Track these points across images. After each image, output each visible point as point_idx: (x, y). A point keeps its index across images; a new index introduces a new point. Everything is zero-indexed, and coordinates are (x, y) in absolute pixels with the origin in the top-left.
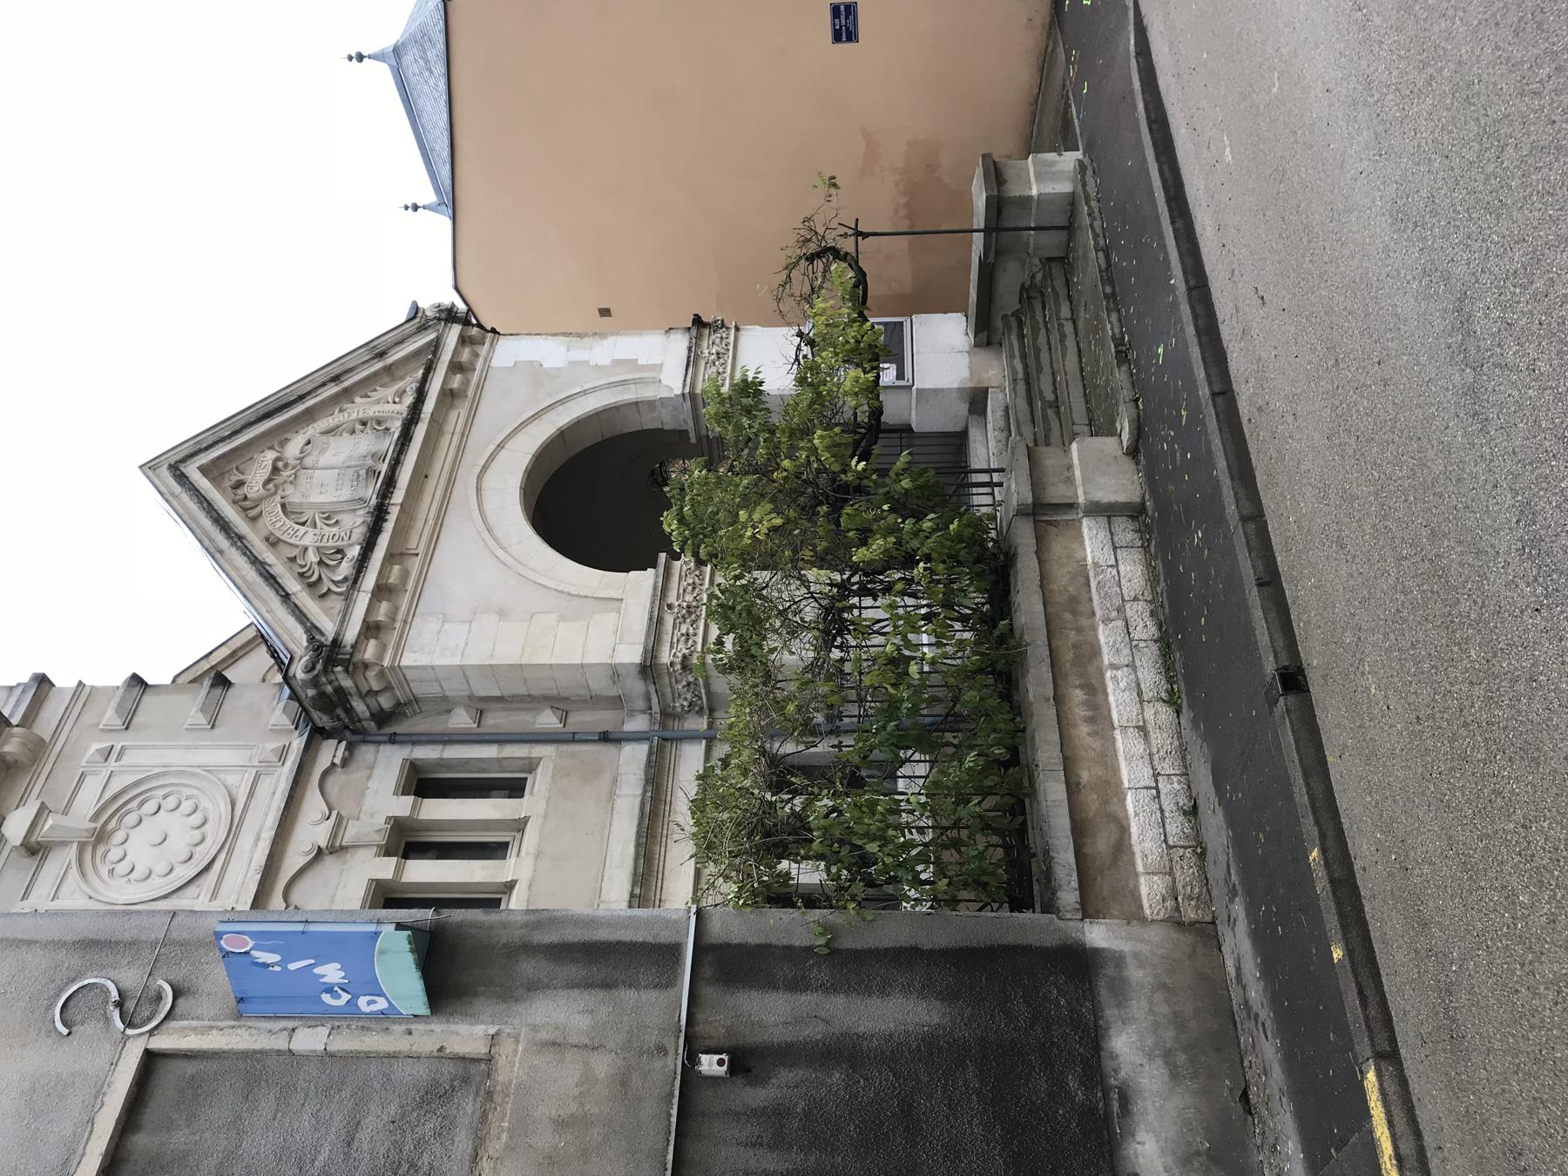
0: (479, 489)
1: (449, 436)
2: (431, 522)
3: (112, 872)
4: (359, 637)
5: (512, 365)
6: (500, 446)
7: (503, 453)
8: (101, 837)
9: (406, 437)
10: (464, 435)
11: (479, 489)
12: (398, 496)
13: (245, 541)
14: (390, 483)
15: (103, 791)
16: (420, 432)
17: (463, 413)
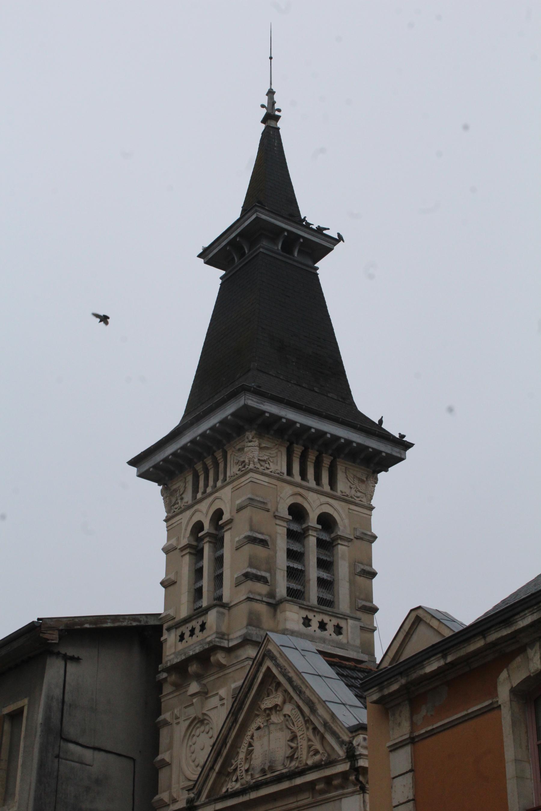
1: (295, 800)
3: (194, 735)
12: (253, 795)
14: (257, 786)
15: (212, 709)
16: (285, 785)
17: (310, 800)
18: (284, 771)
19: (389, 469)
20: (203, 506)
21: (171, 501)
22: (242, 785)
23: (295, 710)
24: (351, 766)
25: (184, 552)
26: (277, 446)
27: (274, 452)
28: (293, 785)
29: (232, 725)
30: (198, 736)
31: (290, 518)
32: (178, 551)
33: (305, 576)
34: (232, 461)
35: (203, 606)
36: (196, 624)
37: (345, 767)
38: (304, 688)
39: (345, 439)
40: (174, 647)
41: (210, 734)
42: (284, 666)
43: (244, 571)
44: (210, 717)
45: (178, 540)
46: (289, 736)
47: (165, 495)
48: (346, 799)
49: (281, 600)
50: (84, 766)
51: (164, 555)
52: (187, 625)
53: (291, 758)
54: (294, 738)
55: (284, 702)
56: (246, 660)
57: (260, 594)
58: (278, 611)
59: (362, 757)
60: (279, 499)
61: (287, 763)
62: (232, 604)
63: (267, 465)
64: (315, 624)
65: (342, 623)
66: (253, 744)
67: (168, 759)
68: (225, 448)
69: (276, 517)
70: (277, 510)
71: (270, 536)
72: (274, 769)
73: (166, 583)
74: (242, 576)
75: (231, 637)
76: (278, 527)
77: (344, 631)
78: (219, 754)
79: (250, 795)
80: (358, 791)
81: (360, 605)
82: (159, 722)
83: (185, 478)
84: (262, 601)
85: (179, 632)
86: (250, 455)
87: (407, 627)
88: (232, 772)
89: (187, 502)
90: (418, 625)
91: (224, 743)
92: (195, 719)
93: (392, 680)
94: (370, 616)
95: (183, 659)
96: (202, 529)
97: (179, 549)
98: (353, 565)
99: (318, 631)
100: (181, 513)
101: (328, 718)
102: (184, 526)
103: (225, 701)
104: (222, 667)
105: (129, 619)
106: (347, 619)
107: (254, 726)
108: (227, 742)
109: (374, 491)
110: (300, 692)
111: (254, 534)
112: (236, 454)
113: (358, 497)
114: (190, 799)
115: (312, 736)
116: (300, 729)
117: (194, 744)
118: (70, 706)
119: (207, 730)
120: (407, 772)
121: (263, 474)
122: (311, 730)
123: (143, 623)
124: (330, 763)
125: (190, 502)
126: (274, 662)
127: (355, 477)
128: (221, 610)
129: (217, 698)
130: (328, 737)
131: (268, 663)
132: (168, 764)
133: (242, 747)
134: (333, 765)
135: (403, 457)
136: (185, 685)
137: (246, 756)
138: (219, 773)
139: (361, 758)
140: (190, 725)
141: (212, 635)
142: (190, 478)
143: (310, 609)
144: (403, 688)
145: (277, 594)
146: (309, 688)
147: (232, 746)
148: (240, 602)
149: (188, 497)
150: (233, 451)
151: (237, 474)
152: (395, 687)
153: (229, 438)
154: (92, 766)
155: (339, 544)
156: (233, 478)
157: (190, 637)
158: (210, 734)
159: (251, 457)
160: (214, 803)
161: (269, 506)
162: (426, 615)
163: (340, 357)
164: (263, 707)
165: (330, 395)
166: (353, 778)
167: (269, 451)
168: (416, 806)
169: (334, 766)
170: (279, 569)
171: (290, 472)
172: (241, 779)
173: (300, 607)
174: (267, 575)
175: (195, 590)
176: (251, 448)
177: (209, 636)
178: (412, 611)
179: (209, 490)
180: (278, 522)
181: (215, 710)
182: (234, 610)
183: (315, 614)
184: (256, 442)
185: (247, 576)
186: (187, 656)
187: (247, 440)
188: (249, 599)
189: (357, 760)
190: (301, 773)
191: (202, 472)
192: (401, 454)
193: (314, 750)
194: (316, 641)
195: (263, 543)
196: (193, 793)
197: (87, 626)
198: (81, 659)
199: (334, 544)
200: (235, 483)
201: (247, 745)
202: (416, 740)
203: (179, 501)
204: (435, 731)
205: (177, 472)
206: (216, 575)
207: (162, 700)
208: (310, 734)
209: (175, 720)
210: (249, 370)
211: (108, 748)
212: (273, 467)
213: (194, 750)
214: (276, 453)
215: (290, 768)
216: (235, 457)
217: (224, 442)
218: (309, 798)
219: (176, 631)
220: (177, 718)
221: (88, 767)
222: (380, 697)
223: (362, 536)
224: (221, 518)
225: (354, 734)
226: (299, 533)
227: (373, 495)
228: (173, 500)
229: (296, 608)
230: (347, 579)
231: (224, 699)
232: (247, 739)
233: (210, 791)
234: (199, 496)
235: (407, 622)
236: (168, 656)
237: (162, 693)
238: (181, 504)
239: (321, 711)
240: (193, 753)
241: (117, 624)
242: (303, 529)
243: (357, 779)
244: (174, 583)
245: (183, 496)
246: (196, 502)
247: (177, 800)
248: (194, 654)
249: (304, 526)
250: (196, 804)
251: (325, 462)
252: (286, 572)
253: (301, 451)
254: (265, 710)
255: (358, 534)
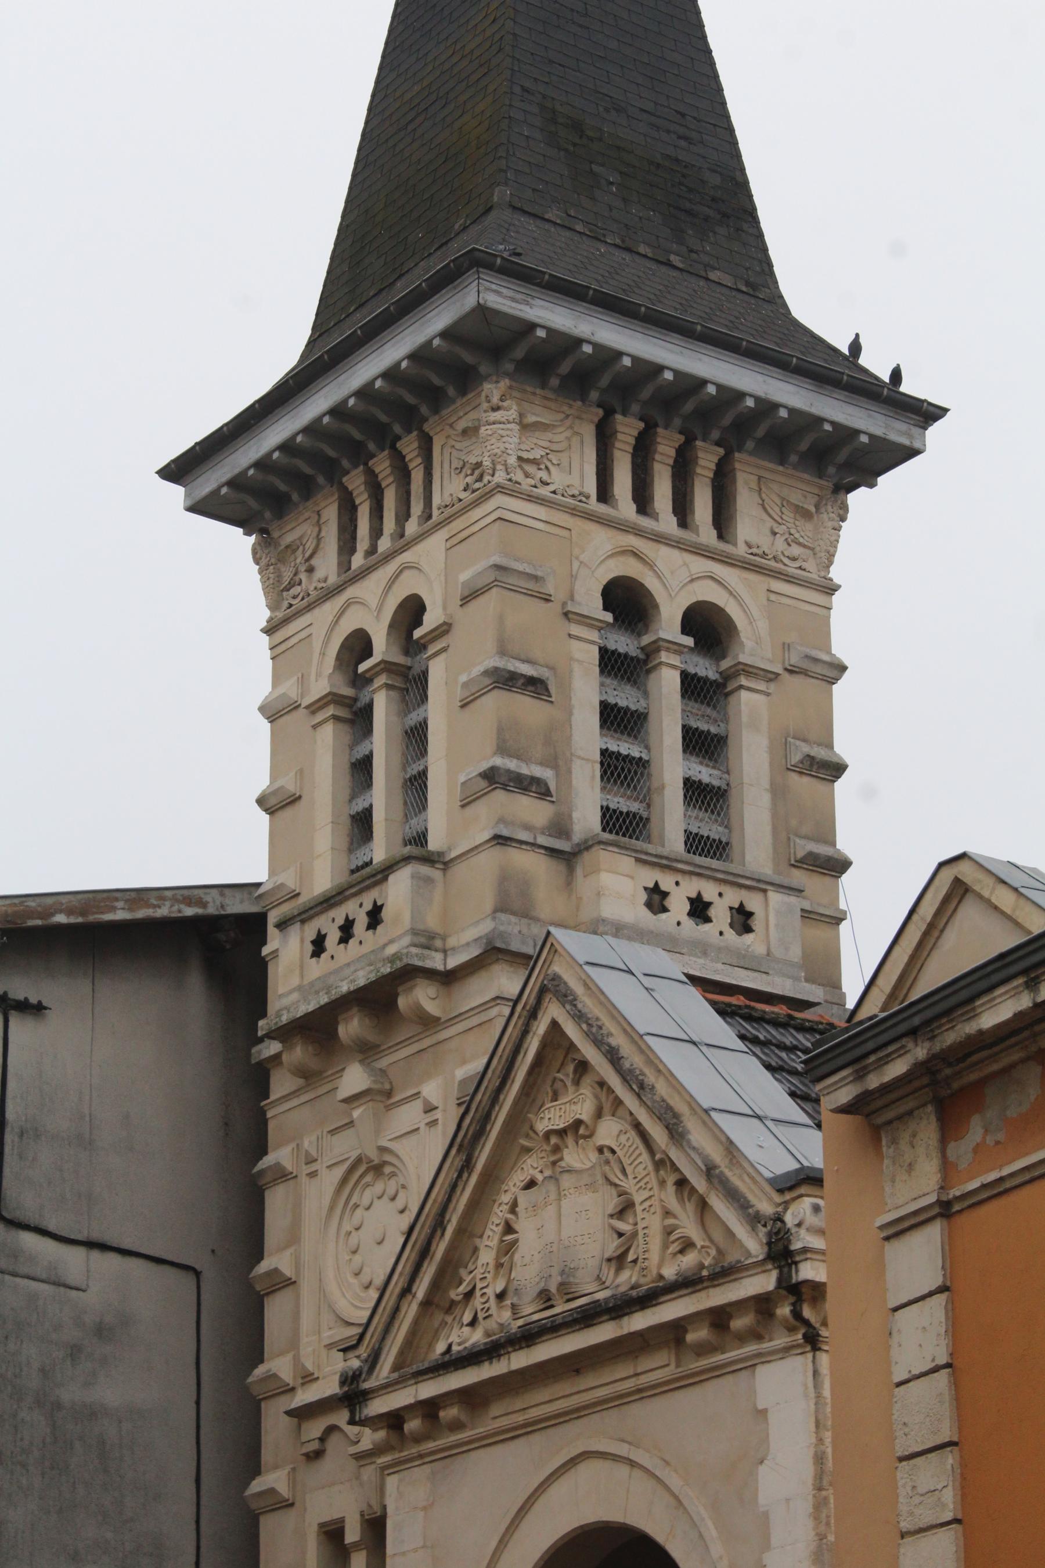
0: (573, 1462)
2: (520, 1418)
3: (356, 1206)
4: (381, 1416)
5: (760, 1407)
6: (632, 1464)
7: (624, 1470)
8: (377, 1169)
9: (588, 1317)
10: (641, 1393)
11: (573, 1462)
12: (520, 1360)
13: (465, 1175)
14: (528, 1337)
16: (604, 1332)
18: (601, 1296)
19: (880, 479)
20: (369, 589)
21: (279, 577)
22: (487, 1334)
23: (628, 1135)
24: (780, 1280)
25: (320, 717)
26: (568, 422)
27: (560, 436)
28: (625, 1331)
29: (460, 1176)
30: (368, 1209)
31: (609, 617)
32: (301, 711)
33: (649, 775)
34: (446, 466)
35: (374, 862)
36: (357, 909)
37: (765, 1282)
38: (651, 1077)
39: (757, 399)
40: (297, 972)
41: (400, 1203)
42: (598, 1019)
43: (484, 766)
44: (397, 1156)
45: (303, 680)
46: (613, 1203)
47: (264, 562)
48: (767, 1366)
49: (586, 841)
50: (62, 1289)
51: (266, 725)
52: (332, 913)
53: (619, 1261)
54: (625, 1209)
55: (599, 1114)
56: (493, 1003)
57: (527, 827)
58: (579, 871)
59: (809, 1255)
60: (576, 565)
61: (609, 1273)
62: (453, 854)
63: (545, 477)
64: (678, 905)
65: (753, 903)
66: (516, 1227)
67: (288, 1271)
68: (426, 427)
69: (570, 616)
70: (572, 598)
71: (552, 668)
72: (573, 1290)
73: (272, 802)
74: (479, 779)
75: (451, 942)
76: (574, 643)
77: (757, 923)
78: (425, 1253)
79: (509, 1359)
80: (798, 1346)
81: (800, 854)
82: (262, 1172)
83: (318, 513)
84: (533, 845)
85: (310, 934)
86: (497, 447)
87: (928, 910)
88: (460, 1302)
89: (325, 580)
90: (960, 902)
91: (439, 1223)
92: (359, 1161)
93: (890, 1049)
94: (827, 880)
95: (322, 1003)
96: (367, 650)
97: (307, 707)
98: (781, 743)
99: (688, 923)
100: (309, 608)
101: (717, 1155)
102: (317, 644)
103: (438, 1115)
104: (428, 1022)
105: (175, 900)
106: (765, 891)
107: (518, 1178)
108: (445, 1222)
109: (838, 541)
110: (642, 1086)
111: (509, 664)
112: (458, 446)
113: (794, 559)
114: (350, 1373)
115: (673, 1203)
116: (642, 1184)
117: (357, 1229)
118: (21, 1135)
119: (391, 1191)
120: (931, 1294)
121: (531, 498)
122: (671, 1188)
123: (211, 910)
124: (724, 1273)
125: (333, 579)
126: (568, 1007)
127: (784, 502)
128: (425, 870)
129: (418, 1105)
130: (718, 1204)
131: (553, 1011)
132: (290, 1283)
133: (485, 1236)
134: (732, 1277)
135: (917, 445)
136: (330, 1072)
137: (497, 1258)
138: (427, 1304)
139: (806, 1259)
140: (344, 1180)
141: (400, 937)
142: (331, 513)
143: (666, 864)
144: (922, 1069)
145: (574, 826)
146: (664, 1075)
147: (460, 1231)
148: (476, 847)
149: (327, 566)
150: (448, 437)
151: (460, 500)
152: (898, 1068)
153: (437, 399)
154: (84, 1291)
155: (741, 687)
156: (449, 511)
157: (342, 946)
158: (400, 1203)
159: (500, 453)
160: (413, 1381)
161: (550, 588)
162: (981, 876)
163: (742, 169)
164: (542, 1127)
165: (714, 275)
166: (784, 1311)
167: (549, 435)
168: (956, 1384)
169: (736, 1280)
170: (579, 757)
171: (604, 494)
172: (485, 1318)
173: (638, 860)
174: (546, 774)
175: (353, 817)
176: (501, 426)
177: (391, 942)
178: (941, 865)
179: (384, 544)
180: (576, 630)
181: (413, 1139)
182: (459, 871)
183: (679, 877)
184: (512, 411)
185: (491, 776)
186: (335, 994)
187: (485, 405)
188: (500, 840)
189: (796, 1263)
190: (647, 1300)
191: (365, 496)
192: (910, 437)
193: (680, 1241)
194: (683, 951)
195: (535, 686)
196: (358, 1357)
197: (61, 919)
198: (46, 1008)
199: (729, 689)
200: (458, 524)
201: (500, 1228)
202: (957, 1207)
203: (303, 576)
204: (1008, 1185)
205: (295, 497)
206: (408, 776)
207: (269, 1115)
208: (670, 1196)
209: (304, 1167)
210: (489, 210)
211: (126, 1244)
212: (558, 479)
213: (359, 1245)
214: (568, 439)
215: (618, 1286)
216: (455, 453)
217: (424, 410)
218: (668, 1365)
219: (302, 930)
220: (310, 1161)
221: (74, 1293)
222: (857, 1096)
223: (806, 665)
224: (418, 622)
225: (788, 1196)
226: (632, 658)
227: (835, 552)
228: (287, 575)
229: (626, 863)
230: (765, 783)
231: (436, 1108)
232: (501, 1214)
233: (401, 1353)
234: (358, 560)
235: (929, 895)
236: (281, 996)
237: (266, 1095)
238: (309, 585)
239: (697, 1136)
240: (355, 1252)
241: (141, 914)
242: (642, 649)
243: (797, 1315)
244: (294, 800)
245: (314, 562)
246: (351, 578)
247: (316, 1376)
248: (352, 989)
249: (646, 640)
250: (366, 1386)
251: (701, 462)
252: (598, 766)
253: (635, 433)
254: (548, 1135)
255: (794, 659)
